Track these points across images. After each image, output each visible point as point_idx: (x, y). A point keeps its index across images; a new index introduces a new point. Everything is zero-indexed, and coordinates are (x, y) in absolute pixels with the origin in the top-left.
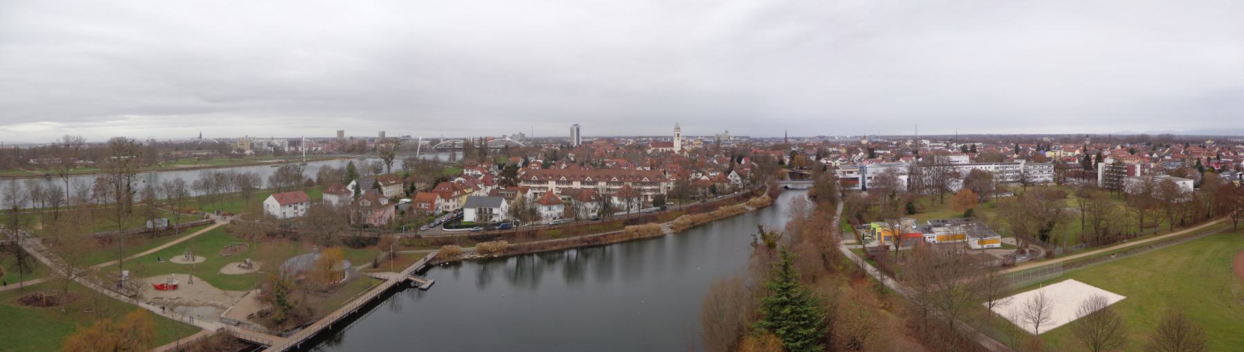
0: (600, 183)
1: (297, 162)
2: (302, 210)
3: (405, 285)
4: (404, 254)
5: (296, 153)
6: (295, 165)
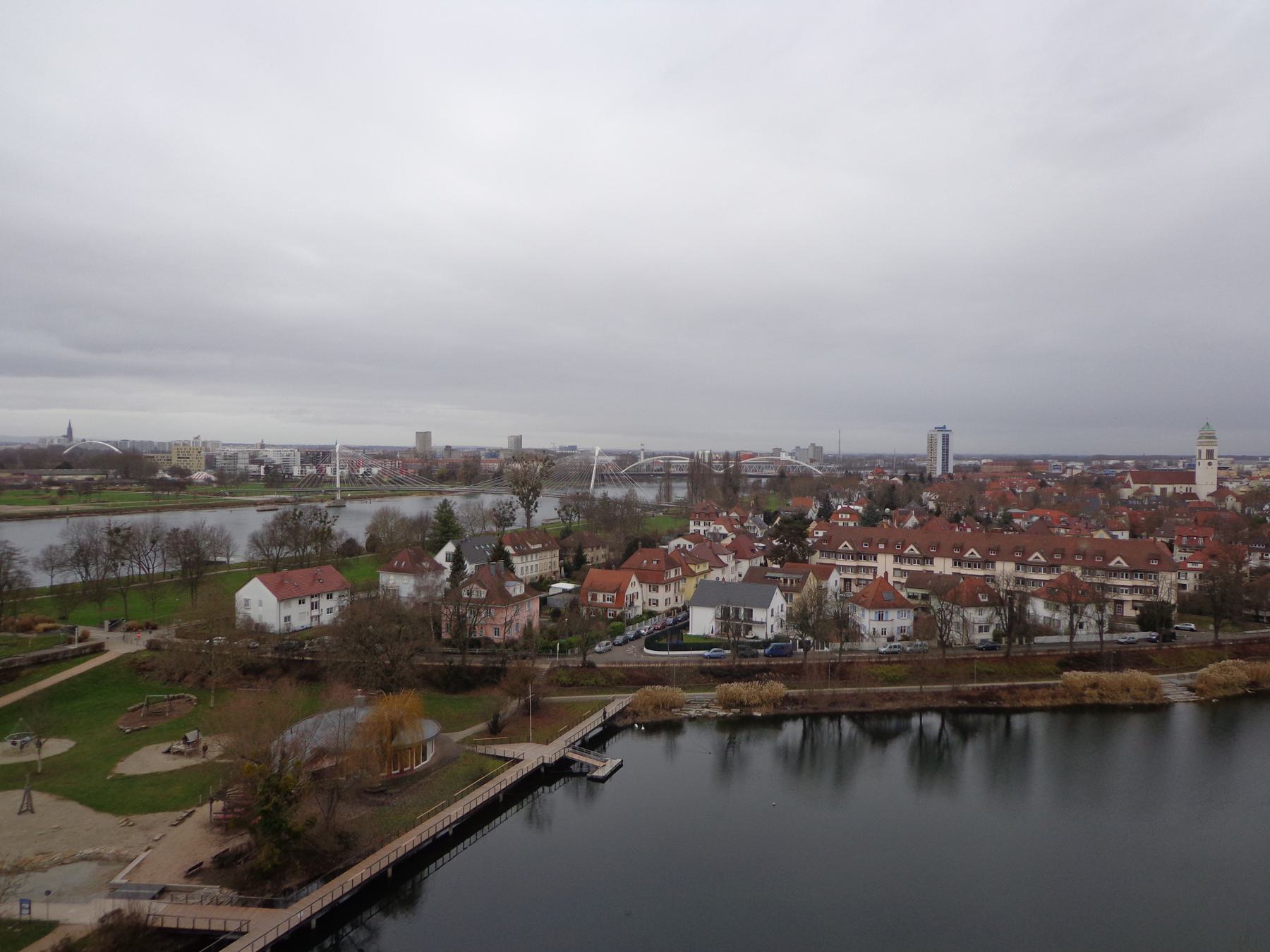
0: (999, 566)
1: (322, 501)
2: (329, 611)
3: (558, 771)
4: (560, 704)
5: (318, 481)
6: (315, 508)
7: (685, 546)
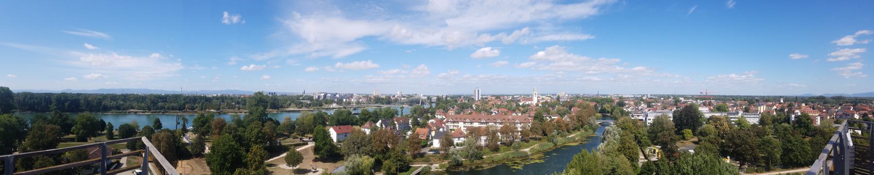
0: (490, 124)
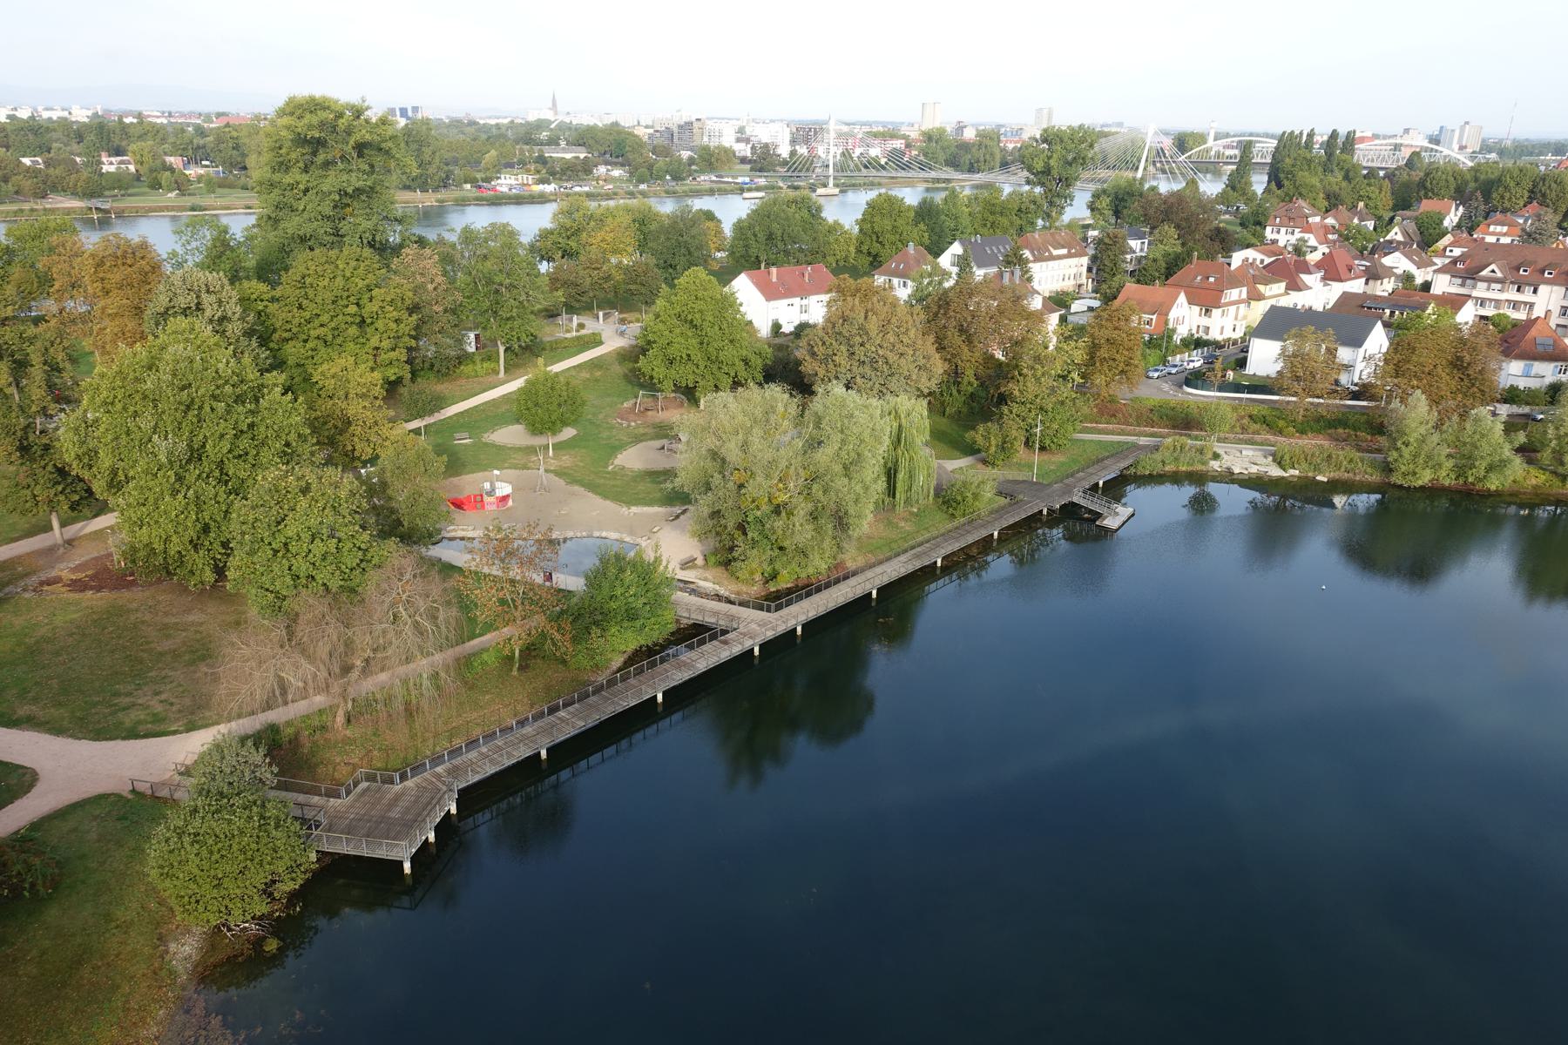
7: (1254, 260)
